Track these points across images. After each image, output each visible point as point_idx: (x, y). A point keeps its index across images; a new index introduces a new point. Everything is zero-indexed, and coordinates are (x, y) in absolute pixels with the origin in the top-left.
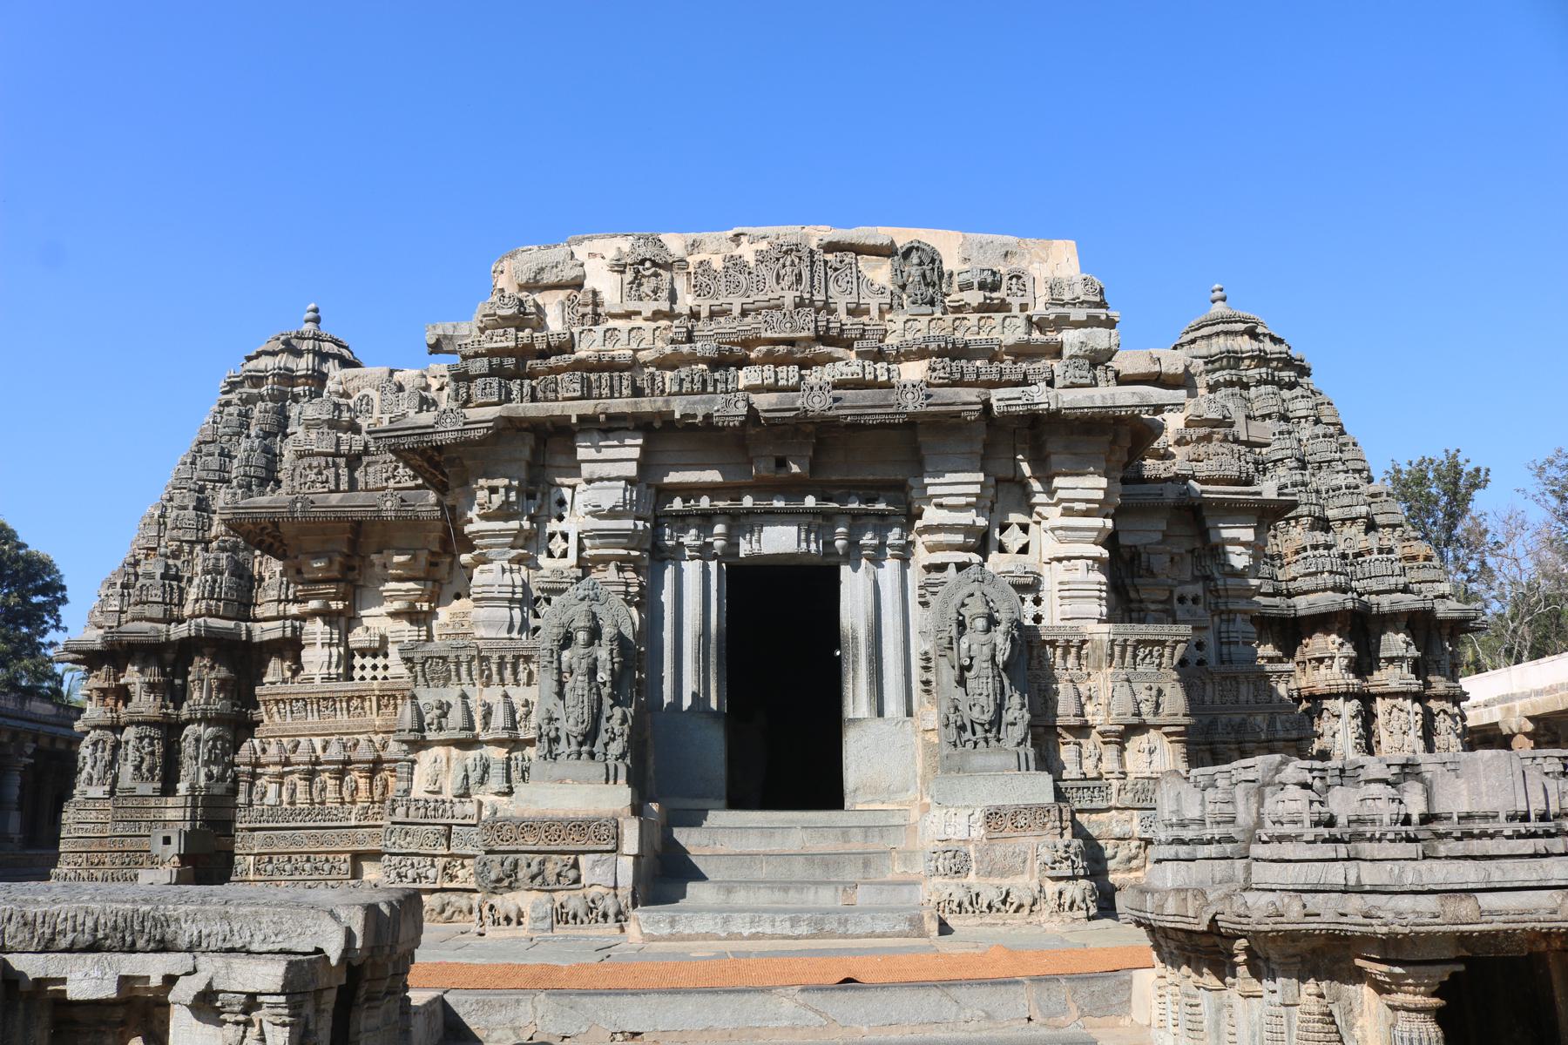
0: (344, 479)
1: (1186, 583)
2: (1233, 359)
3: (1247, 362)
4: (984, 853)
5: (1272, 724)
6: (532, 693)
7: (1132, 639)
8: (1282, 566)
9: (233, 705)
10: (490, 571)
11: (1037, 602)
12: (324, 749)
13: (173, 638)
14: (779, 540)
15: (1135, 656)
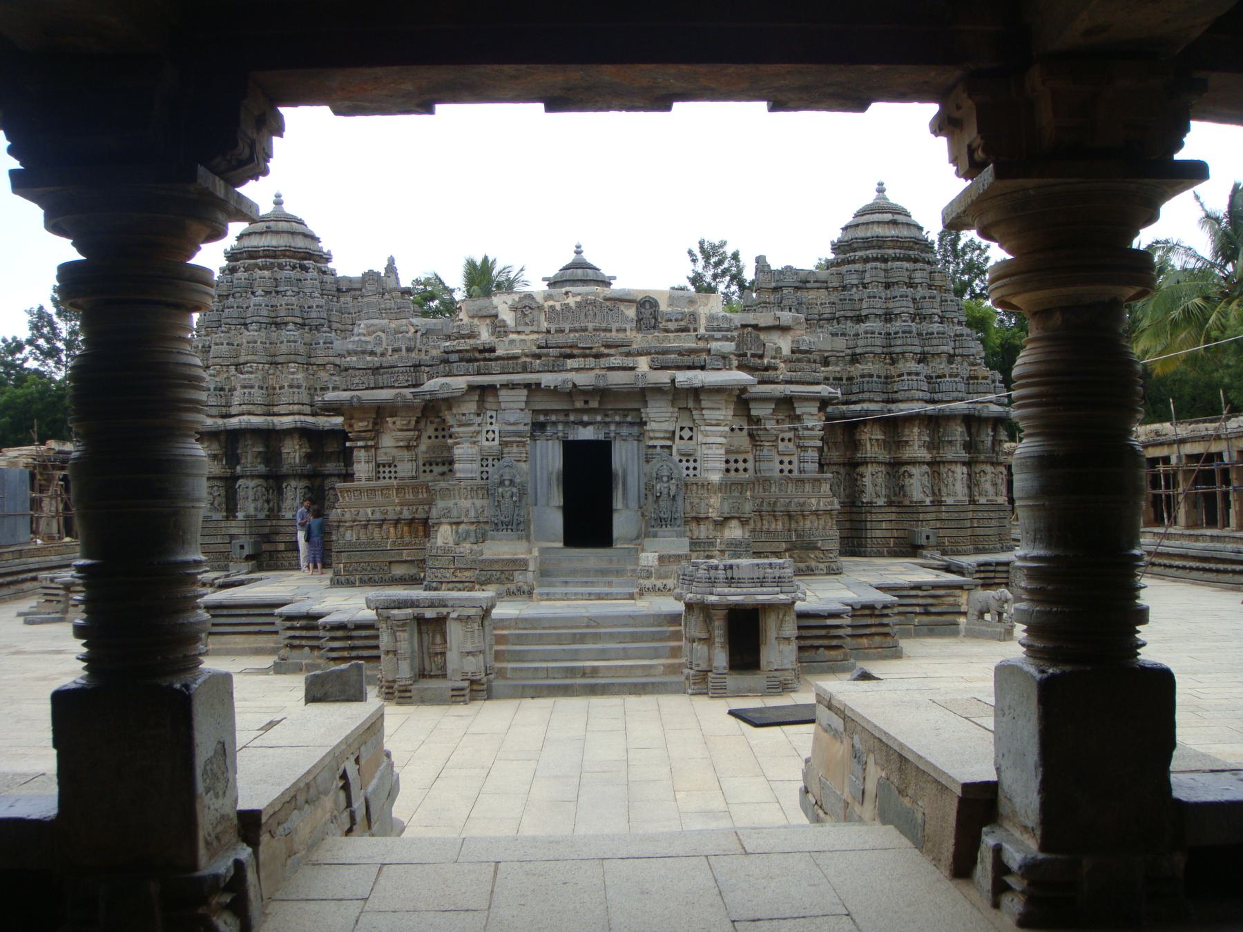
0: (372, 381)
1: (785, 431)
2: (879, 242)
3: (889, 244)
4: (657, 570)
5: (818, 504)
6: (485, 502)
7: (729, 483)
8: (892, 382)
9: (266, 467)
10: (461, 448)
11: (695, 461)
12: (372, 514)
13: (229, 428)
14: (586, 434)
15: (730, 489)
